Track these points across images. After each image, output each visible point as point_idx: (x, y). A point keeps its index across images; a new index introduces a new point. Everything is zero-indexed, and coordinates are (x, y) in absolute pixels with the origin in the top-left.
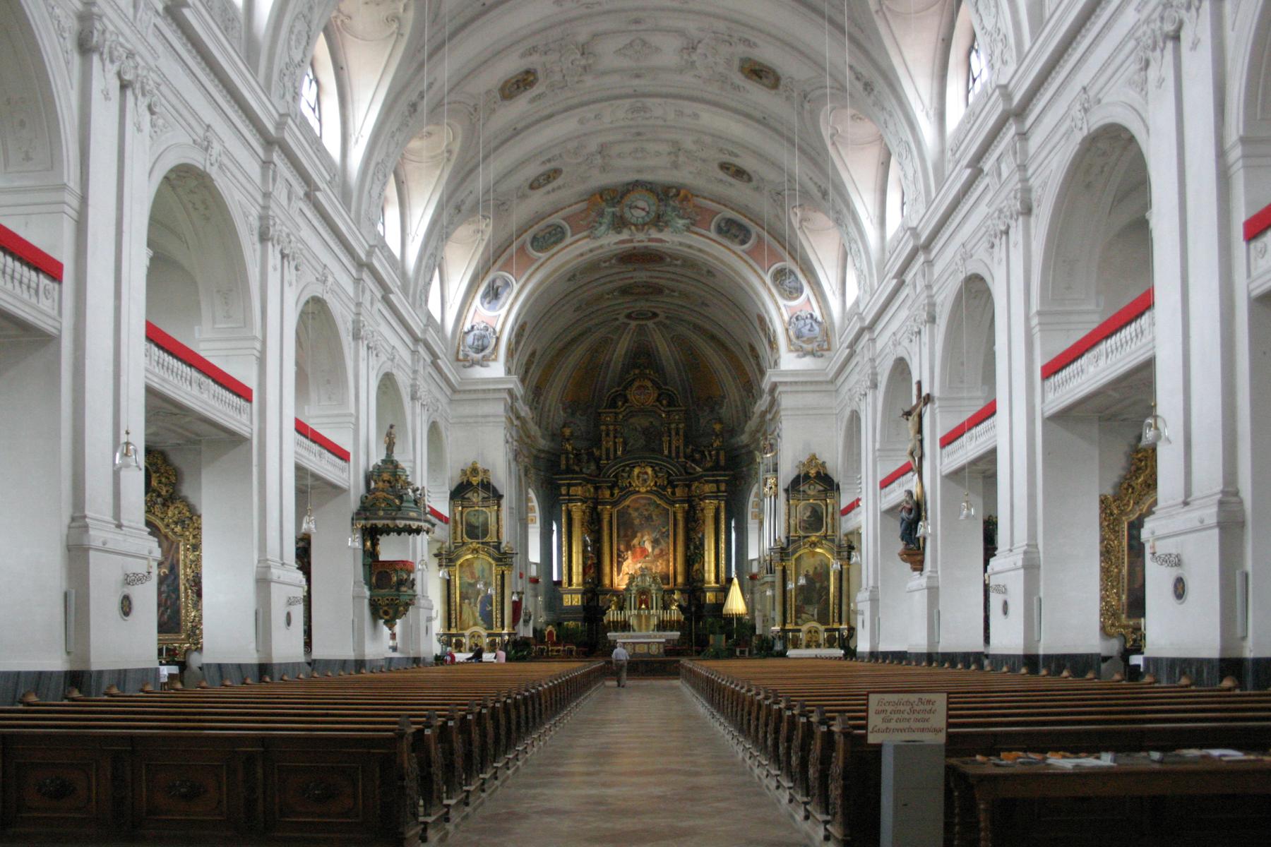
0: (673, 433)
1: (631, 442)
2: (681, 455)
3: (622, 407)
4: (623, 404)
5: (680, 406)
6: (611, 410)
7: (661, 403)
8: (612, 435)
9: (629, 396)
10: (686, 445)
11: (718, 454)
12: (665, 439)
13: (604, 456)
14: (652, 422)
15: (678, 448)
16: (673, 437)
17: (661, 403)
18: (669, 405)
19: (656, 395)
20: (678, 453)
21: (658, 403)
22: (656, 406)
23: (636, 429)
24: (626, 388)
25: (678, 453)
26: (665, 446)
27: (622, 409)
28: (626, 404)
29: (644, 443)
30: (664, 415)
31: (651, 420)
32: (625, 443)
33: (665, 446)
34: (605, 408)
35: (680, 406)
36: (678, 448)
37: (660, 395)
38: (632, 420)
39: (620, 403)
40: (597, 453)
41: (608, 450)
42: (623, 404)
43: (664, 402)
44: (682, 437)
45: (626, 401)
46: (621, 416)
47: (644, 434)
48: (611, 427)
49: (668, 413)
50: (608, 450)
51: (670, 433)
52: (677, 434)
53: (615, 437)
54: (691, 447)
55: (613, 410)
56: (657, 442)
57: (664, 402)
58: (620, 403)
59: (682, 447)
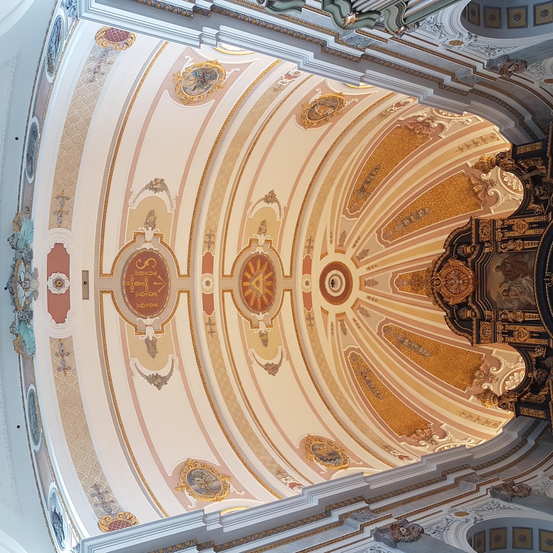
0: (511, 234)
1: (526, 298)
2: (543, 218)
3: (473, 310)
4: (470, 308)
5: (470, 229)
6: (474, 327)
7: (469, 255)
8: (511, 328)
9: (460, 300)
10: (531, 213)
11: (526, 156)
12: (518, 246)
13: (544, 342)
14: (497, 267)
15: (531, 226)
16: (517, 234)
17: (469, 255)
18: (469, 243)
19: (461, 264)
20: (541, 225)
21: (469, 260)
22: (473, 261)
23: (508, 291)
24: (446, 304)
25: (541, 225)
26: (529, 245)
27: (477, 311)
28: (470, 304)
29: (528, 277)
30: (487, 250)
31: (494, 270)
32: (526, 308)
33: (529, 245)
34: (471, 334)
35: (470, 229)
36: (531, 226)
37: (460, 258)
38: (494, 297)
39: (469, 314)
40: (541, 353)
41: (532, 335)
42: (470, 308)
43: (468, 250)
44: (516, 220)
45: (463, 305)
46: (487, 312)
47: (514, 278)
48: (500, 327)
49: (482, 244)
50: (532, 335)
51: (509, 239)
52: (510, 228)
53: (516, 322)
54: (532, 206)
55: (474, 323)
56: (527, 256)
57: (468, 250)
58: (469, 314)
59: (531, 220)
